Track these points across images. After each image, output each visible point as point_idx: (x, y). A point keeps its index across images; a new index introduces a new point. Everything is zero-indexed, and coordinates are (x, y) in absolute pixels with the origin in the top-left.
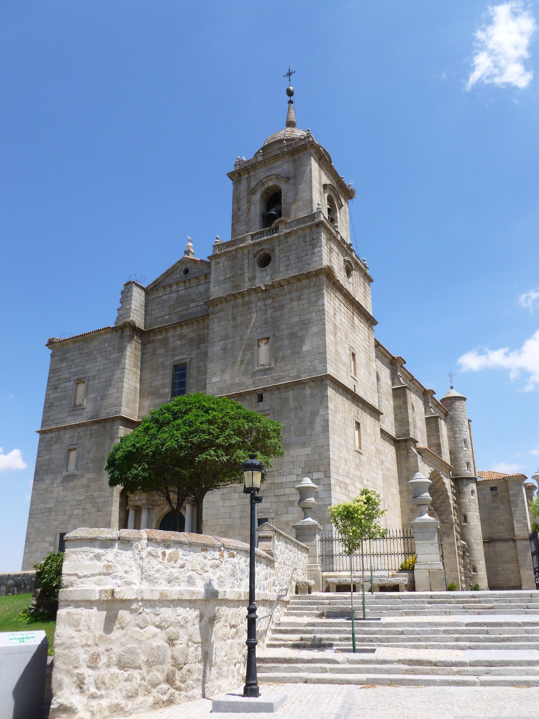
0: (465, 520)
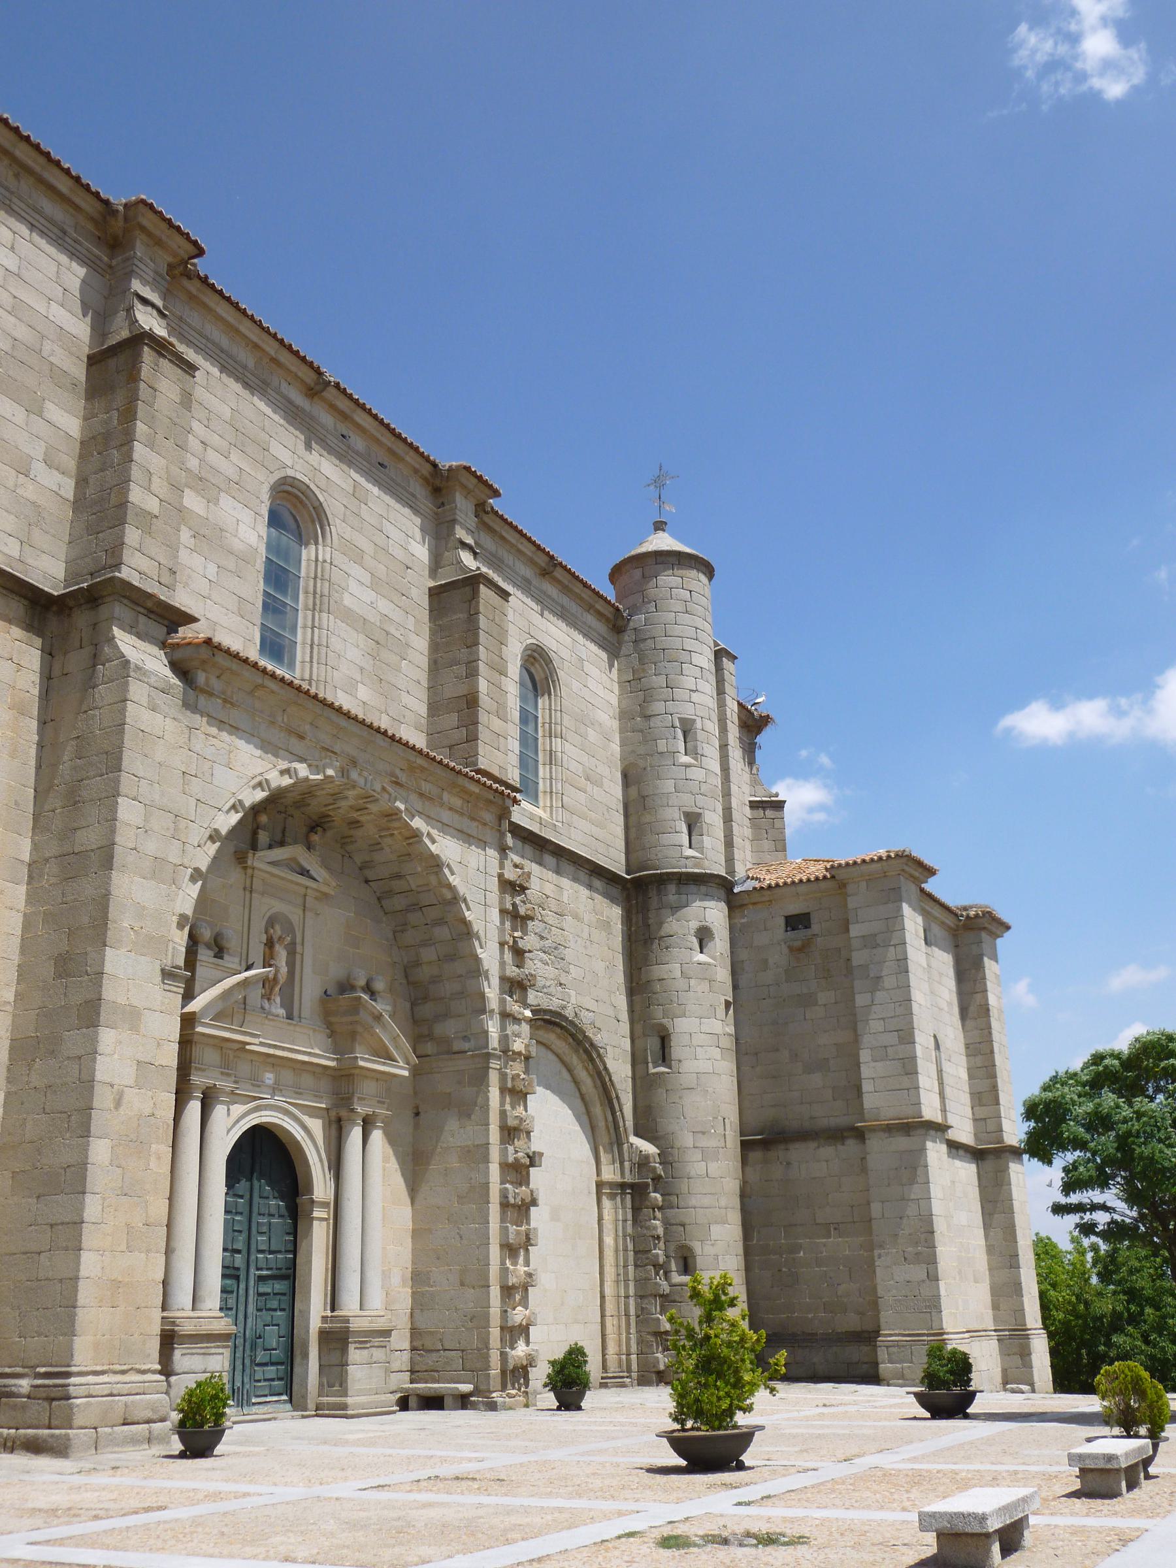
0: (664, 1056)
